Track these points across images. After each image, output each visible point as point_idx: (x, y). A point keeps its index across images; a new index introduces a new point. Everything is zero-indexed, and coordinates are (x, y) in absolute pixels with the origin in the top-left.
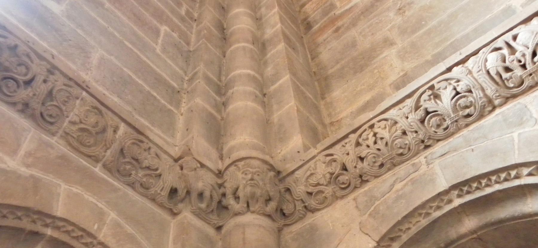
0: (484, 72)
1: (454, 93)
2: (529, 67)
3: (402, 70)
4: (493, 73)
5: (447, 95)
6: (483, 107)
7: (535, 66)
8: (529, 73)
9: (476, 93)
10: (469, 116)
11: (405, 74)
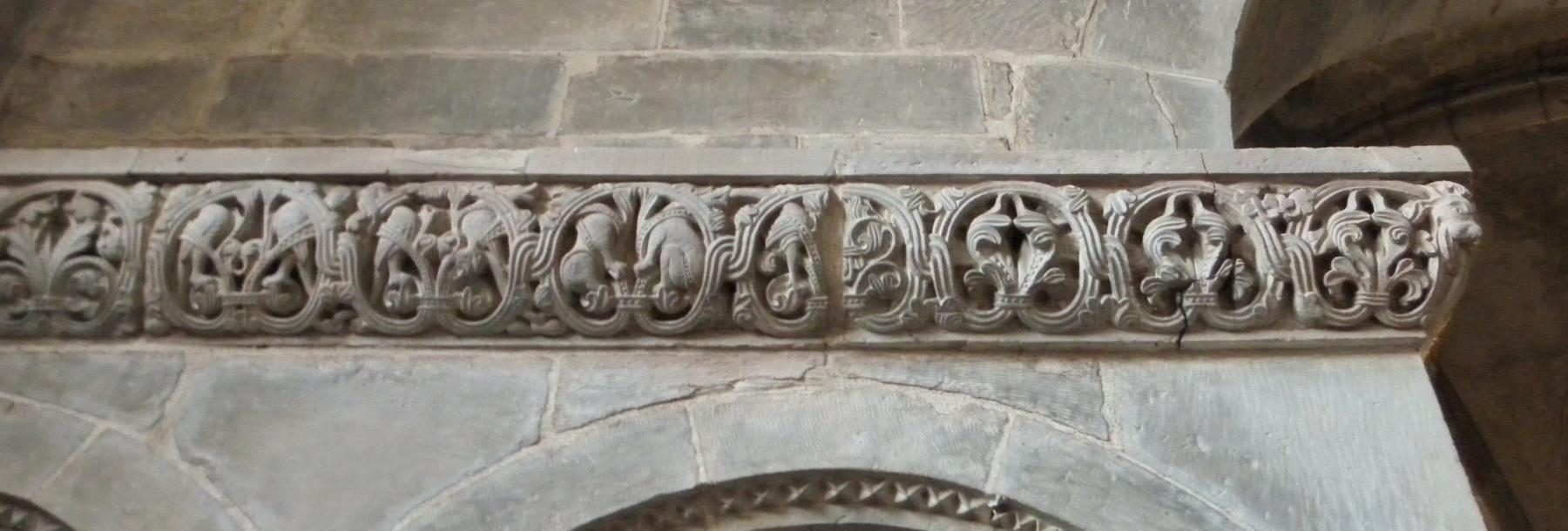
0: (169, 241)
1: (83, 245)
2: (246, 291)
3: (284, 44)
4: (182, 255)
5: (76, 235)
6: (119, 317)
7: (256, 294)
8: (238, 302)
9: (123, 276)
10: (79, 316)
11: (278, 60)
